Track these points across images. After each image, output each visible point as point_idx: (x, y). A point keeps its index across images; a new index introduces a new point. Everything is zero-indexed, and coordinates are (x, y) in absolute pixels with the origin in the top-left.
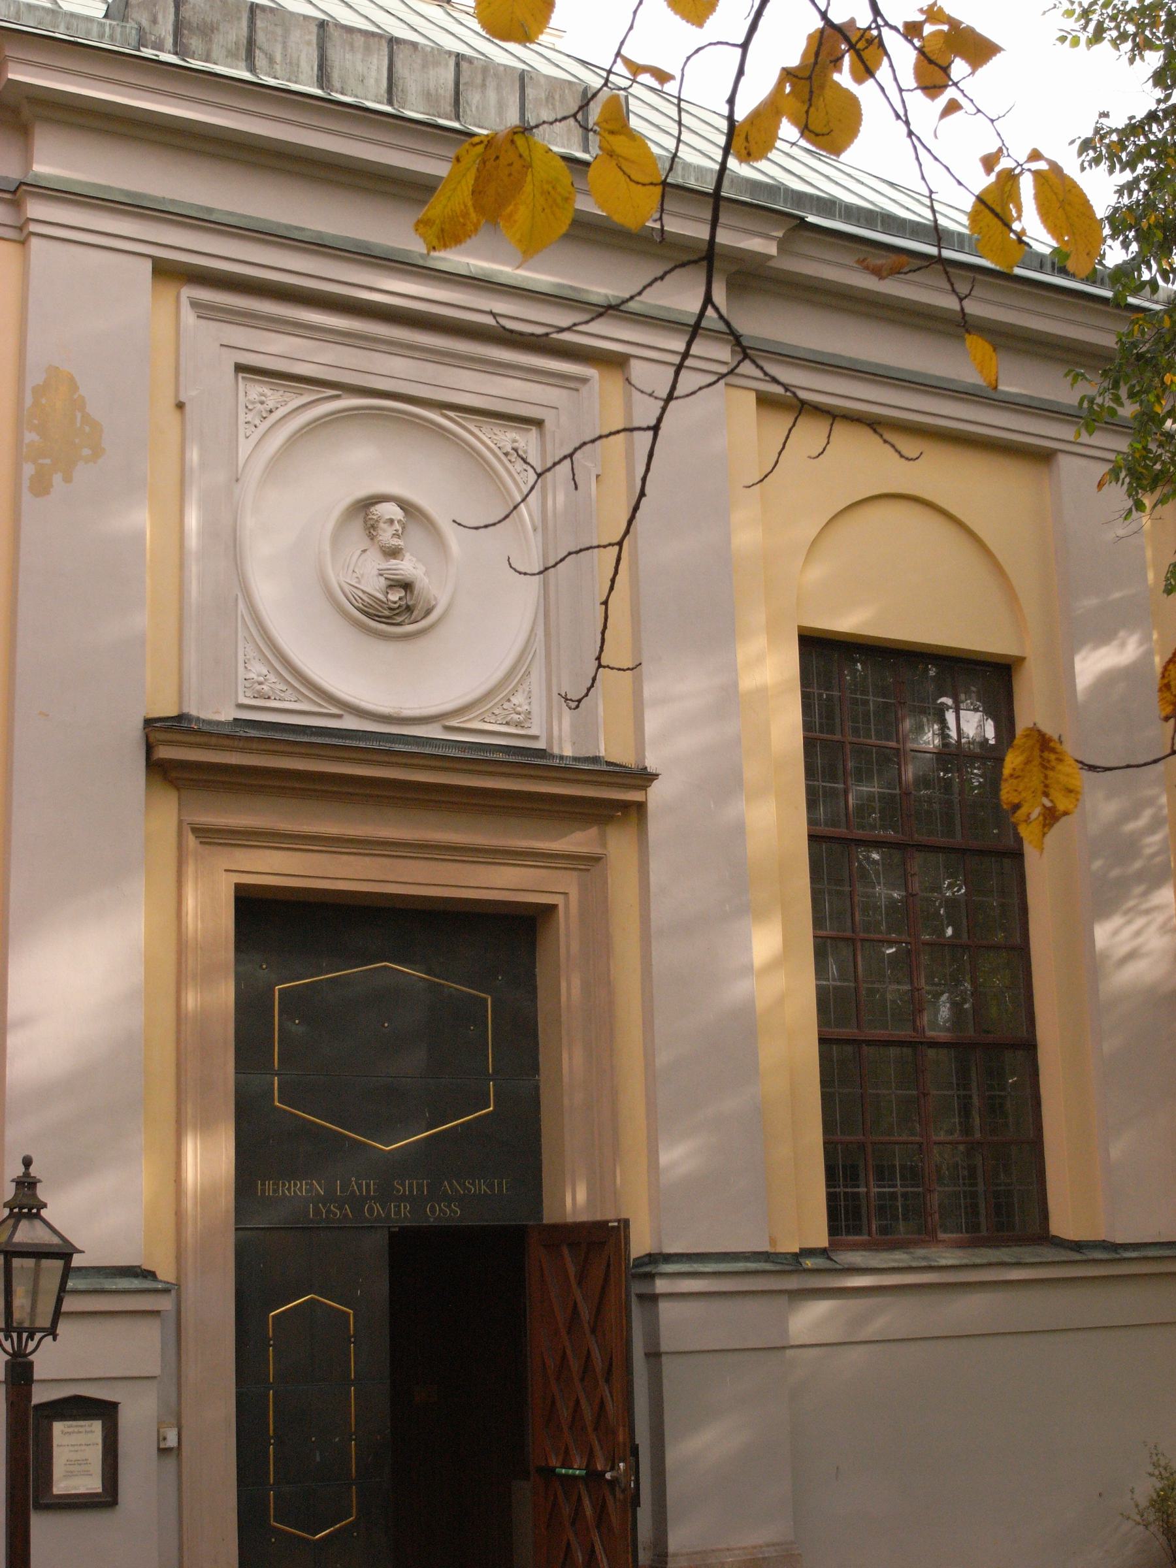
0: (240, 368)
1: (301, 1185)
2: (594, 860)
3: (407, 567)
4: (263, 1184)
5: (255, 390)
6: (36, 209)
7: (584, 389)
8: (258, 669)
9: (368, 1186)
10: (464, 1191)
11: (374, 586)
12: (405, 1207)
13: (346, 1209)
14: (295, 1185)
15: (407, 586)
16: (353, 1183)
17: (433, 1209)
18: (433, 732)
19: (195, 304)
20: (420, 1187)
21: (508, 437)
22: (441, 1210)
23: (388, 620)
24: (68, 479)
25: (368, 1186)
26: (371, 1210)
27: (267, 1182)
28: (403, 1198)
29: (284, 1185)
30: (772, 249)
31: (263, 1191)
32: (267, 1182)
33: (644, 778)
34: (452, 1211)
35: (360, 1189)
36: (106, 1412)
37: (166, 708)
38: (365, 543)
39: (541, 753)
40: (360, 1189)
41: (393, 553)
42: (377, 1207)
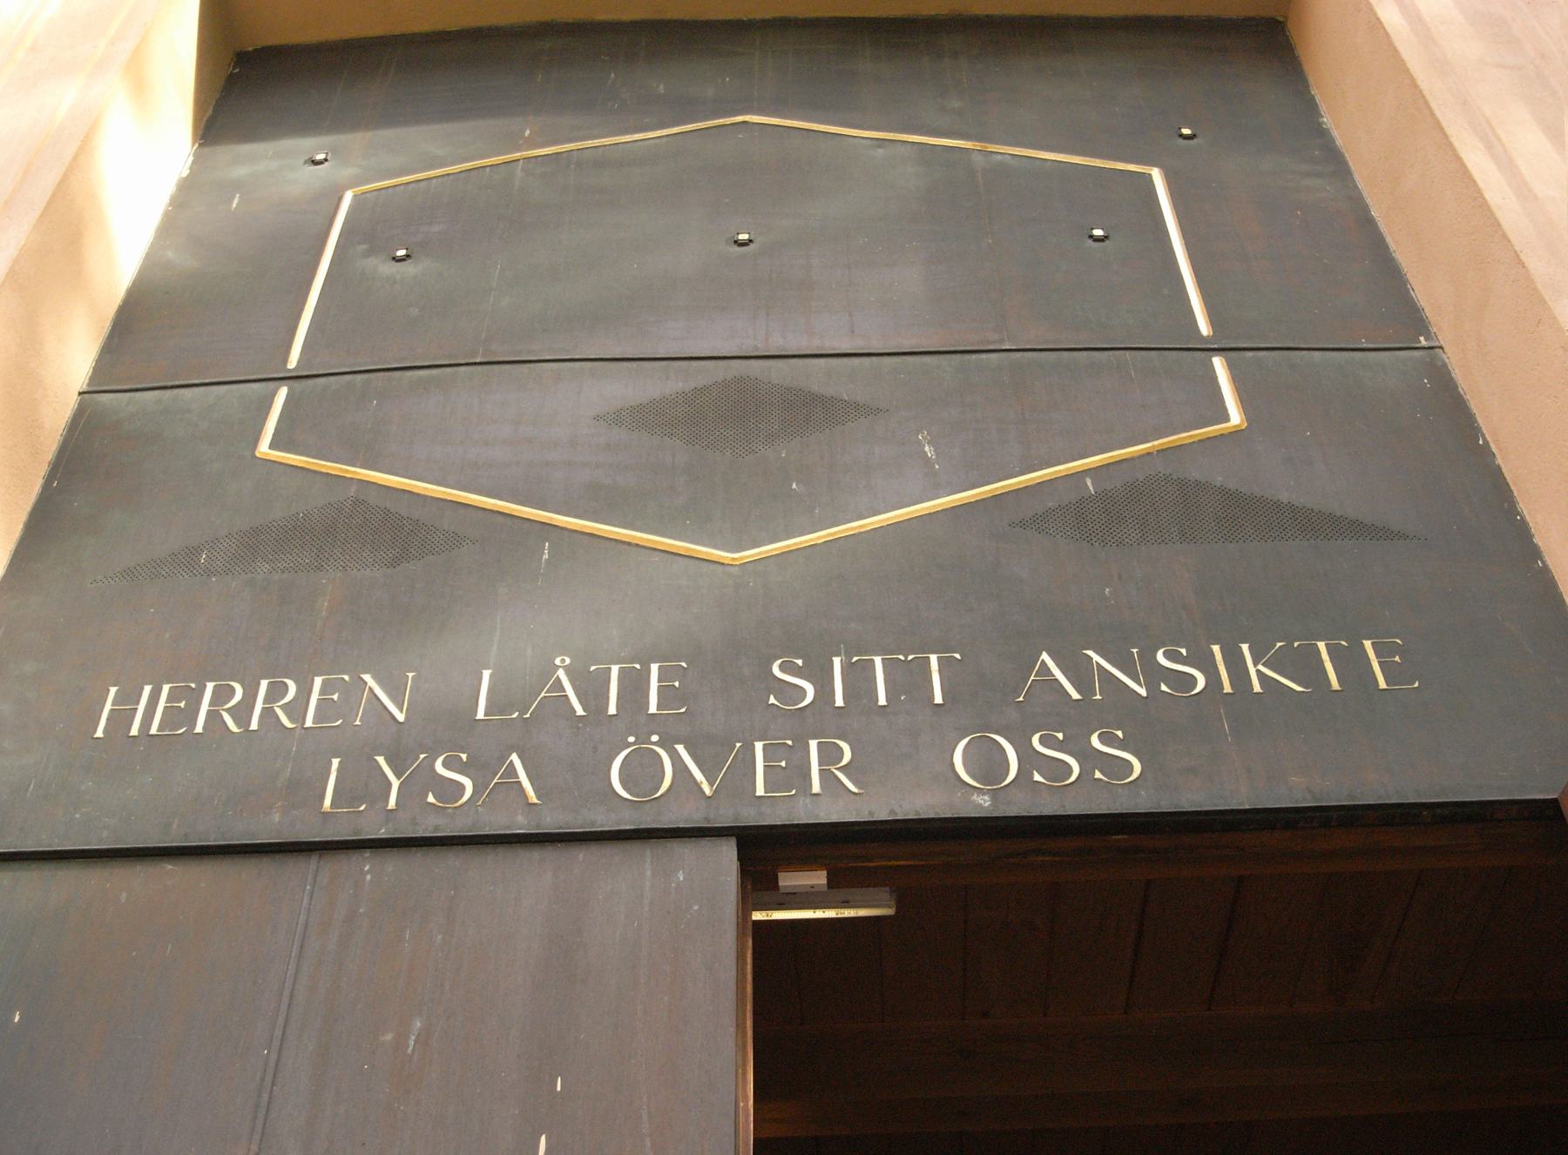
1: (304, 692)
4: (129, 697)
9: (634, 687)
10: (1152, 686)
12: (830, 755)
13: (511, 771)
14: (276, 691)
16: (561, 673)
17: (988, 765)
20: (909, 681)
22: (1029, 758)
25: (634, 687)
26: (642, 771)
27: (147, 689)
28: (820, 719)
29: (222, 695)
31: (121, 719)
32: (147, 689)
34: (1089, 758)
35: (593, 691)
40: (593, 691)
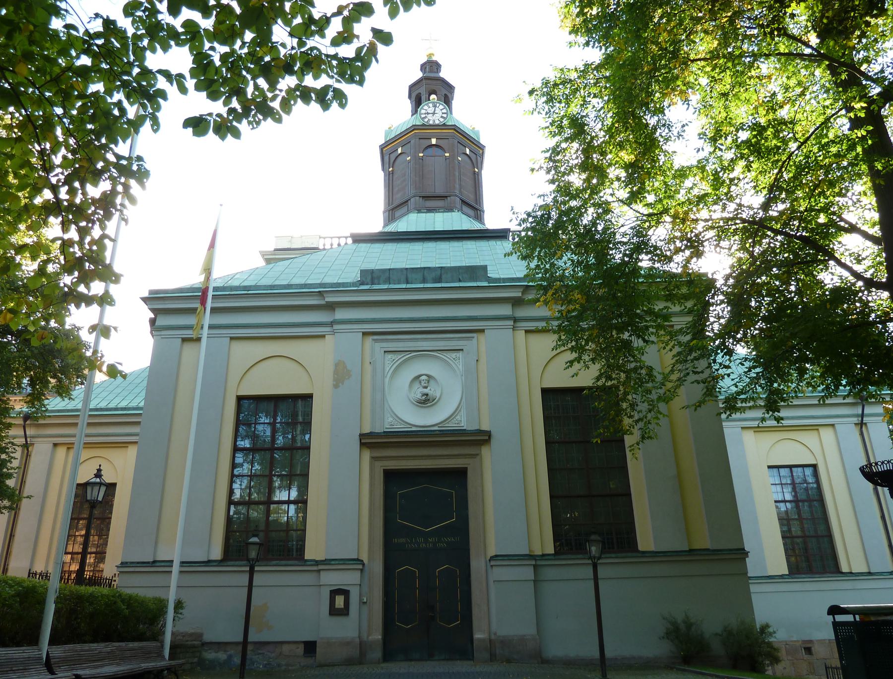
0: (385, 352)
2: (477, 455)
3: (426, 391)
5: (390, 356)
6: (335, 327)
7: (474, 339)
8: (390, 419)
11: (419, 396)
15: (427, 395)
18: (436, 428)
19: (373, 340)
21: (454, 355)
23: (424, 403)
24: (343, 384)
30: (520, 294)
33: (488, 434)
36: (346, 593)
37: (367, 430)
38: (419, 386)
39: (465, 430)
41: (426, 387)
42: (424, 545)
